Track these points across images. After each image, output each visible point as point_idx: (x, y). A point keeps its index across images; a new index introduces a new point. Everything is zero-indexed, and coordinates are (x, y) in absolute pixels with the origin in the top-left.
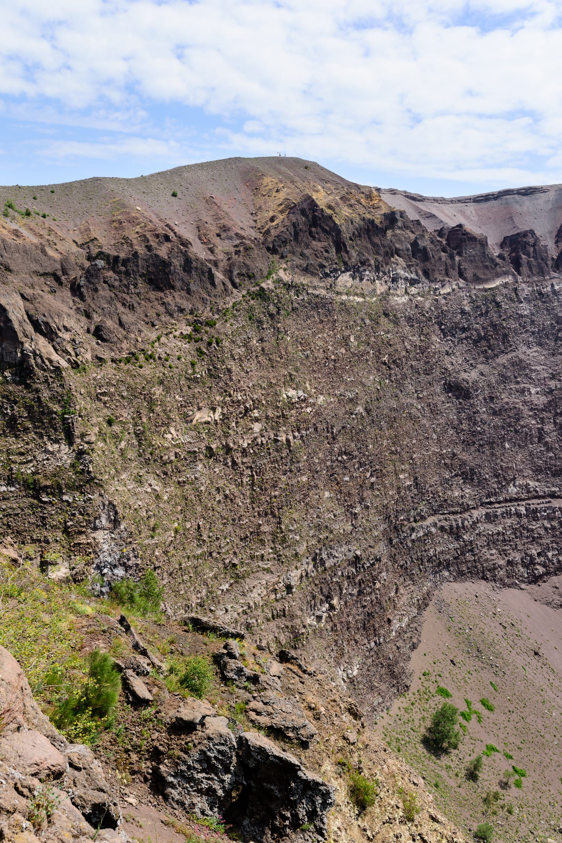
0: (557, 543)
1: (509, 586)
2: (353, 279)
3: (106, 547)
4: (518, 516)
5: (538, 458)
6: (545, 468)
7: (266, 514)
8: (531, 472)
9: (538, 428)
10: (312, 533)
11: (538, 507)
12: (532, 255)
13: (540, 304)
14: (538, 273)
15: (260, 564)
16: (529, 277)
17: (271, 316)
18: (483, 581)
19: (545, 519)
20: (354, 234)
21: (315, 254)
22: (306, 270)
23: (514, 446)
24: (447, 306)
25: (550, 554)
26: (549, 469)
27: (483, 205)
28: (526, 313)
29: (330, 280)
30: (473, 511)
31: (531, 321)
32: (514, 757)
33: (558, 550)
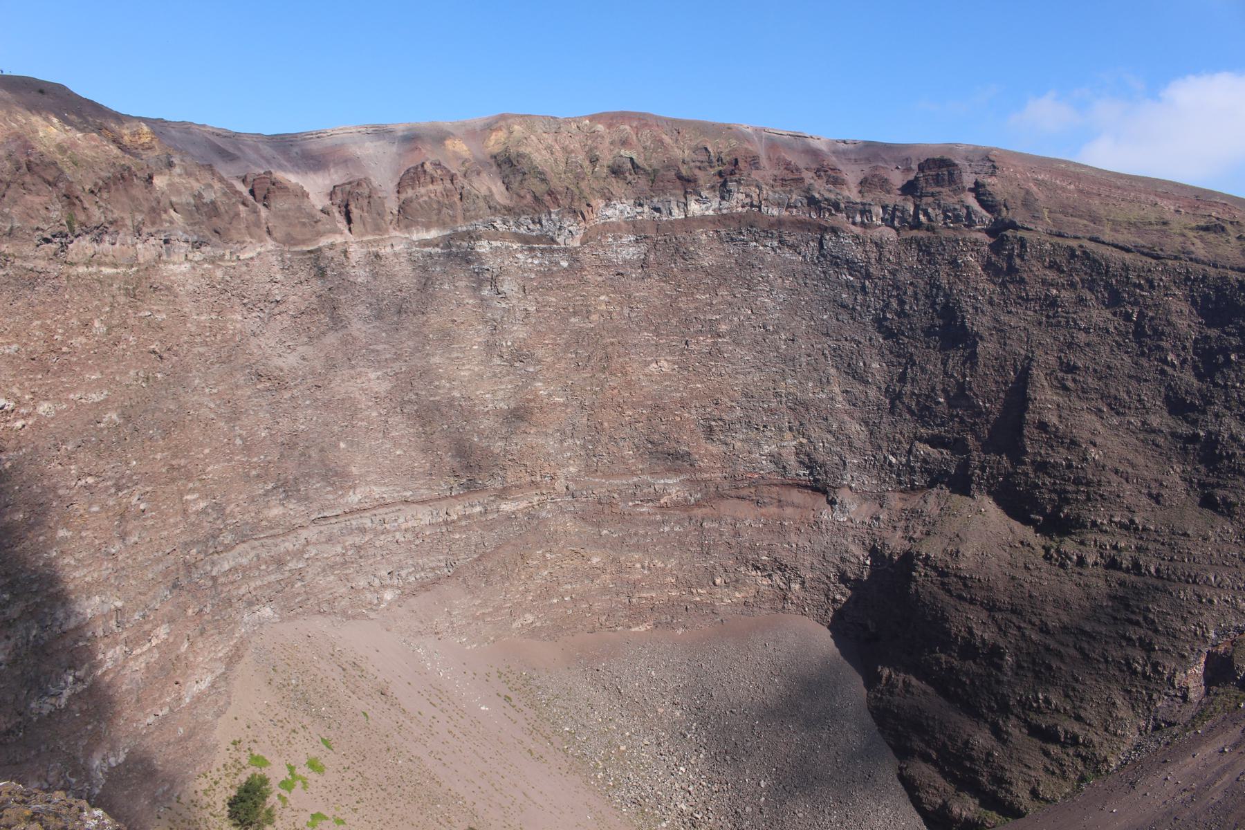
1: (354, 618)
11: (385, 516)
12: (365, 209)
18: (319, 617)
20: (96, 184)
21: (28, 214)
23: (352, 446)
24: (249, 275)
25: (403, 573)
28: (359, 280)
30: (300, 531)
32: (346, 822)
33: (415, 567)
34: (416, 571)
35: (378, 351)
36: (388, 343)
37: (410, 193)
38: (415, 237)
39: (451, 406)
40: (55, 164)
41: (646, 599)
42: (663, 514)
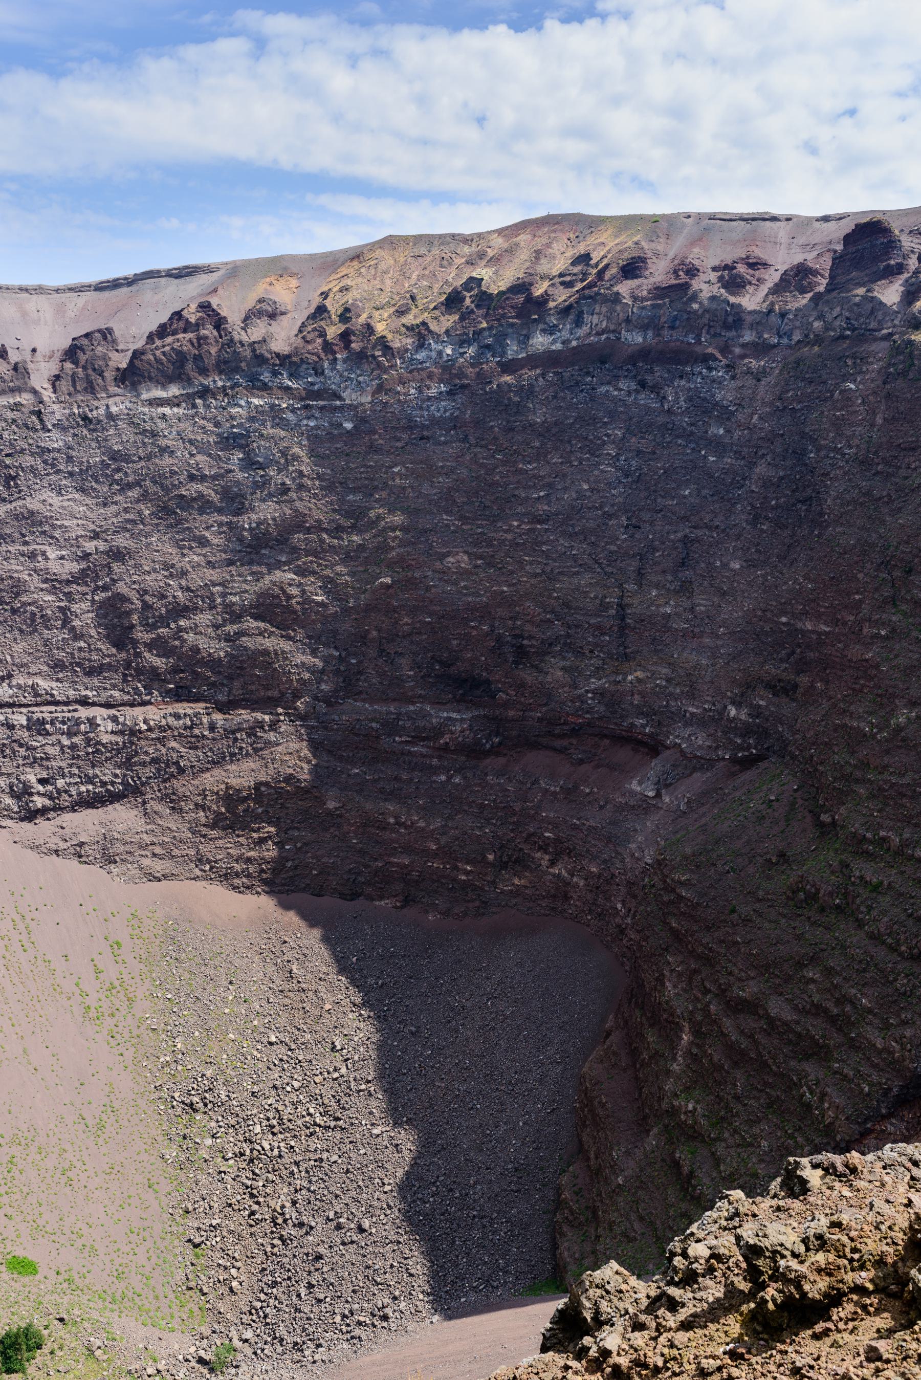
0: (79, 767)
4: (8, 728)
5: (58, 649)
6: (71, 664)
8: (45, 668)
9: (59, 607)
11: (48, 717)
12: (81, 365)
13: (85, 432)
14: (85, 389)
16: (70, 394)
19: (63, 734)
25: (60, 783)
26: (79, 664)
27: (107, 294)
28: (56, 445)
31: (68, 457)
33: (80, 777)
34: (82, 783)
35: (66, 527)
36: (87, 518)
37: (158, 343)
38: (145, 396)
39: (163, 597)
41: (398, 865)
42: (440, 758)
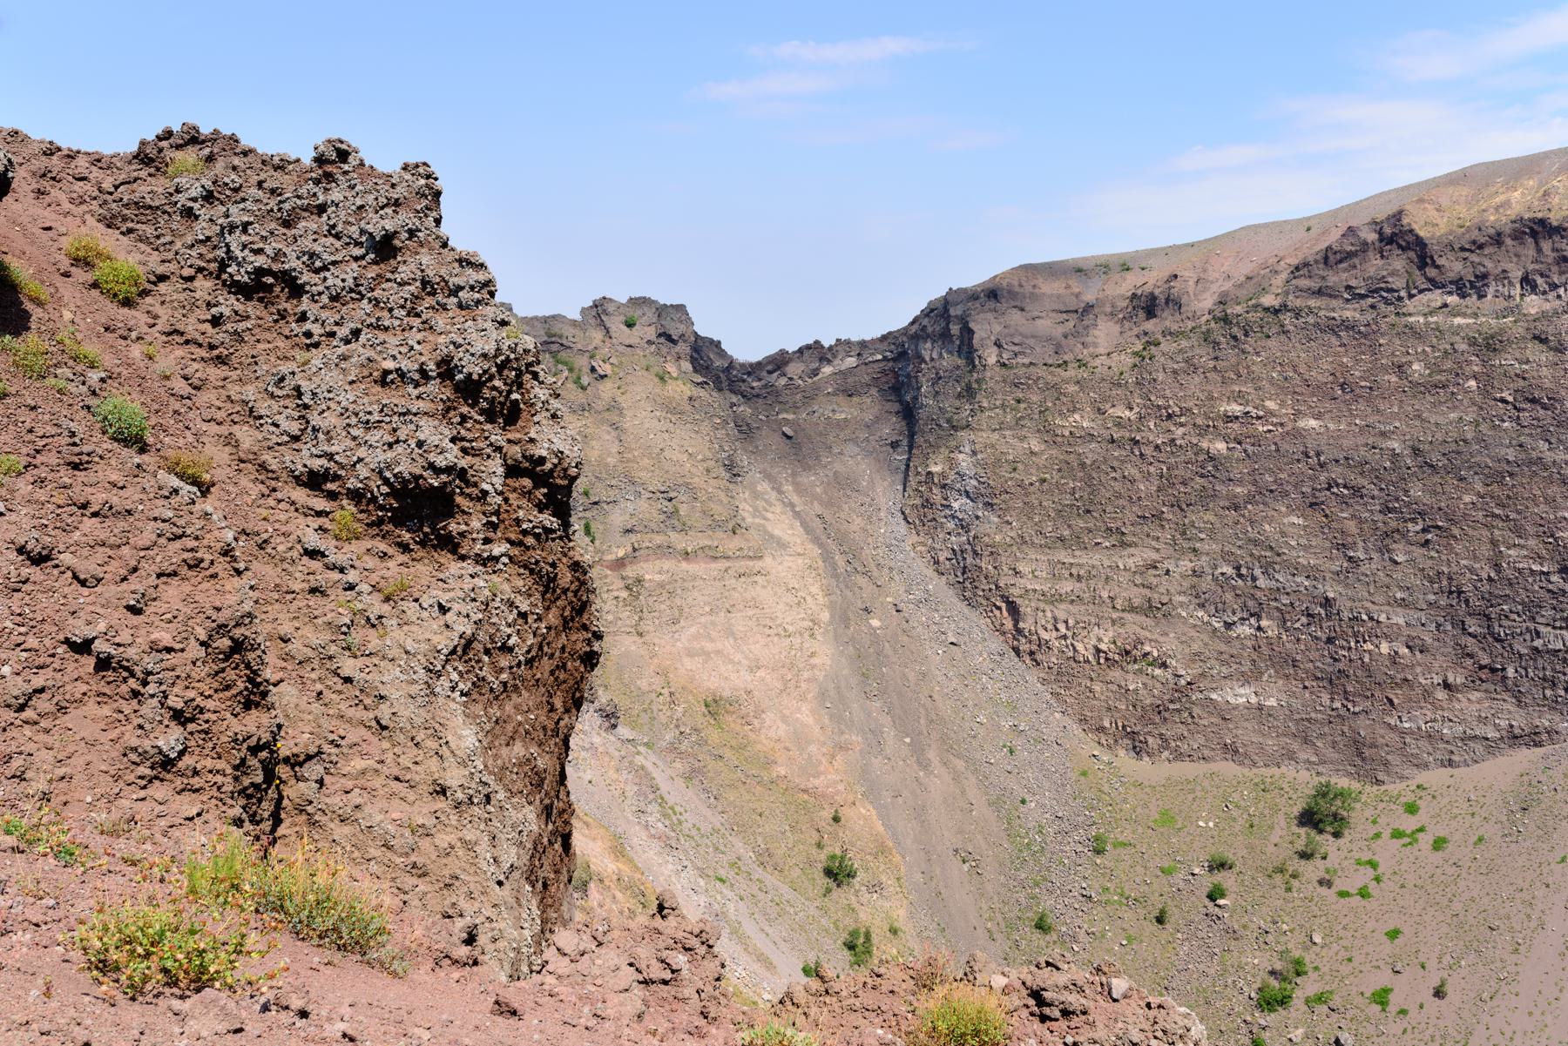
2: (1463, 296)
3: (964, 464)
7: (1172, 506)
10: (1240, 543)
15: (1154, 543)
17: (1235, 338)
22: (1319, 292)
29: (1371, 300)
40: (1411, 231)
